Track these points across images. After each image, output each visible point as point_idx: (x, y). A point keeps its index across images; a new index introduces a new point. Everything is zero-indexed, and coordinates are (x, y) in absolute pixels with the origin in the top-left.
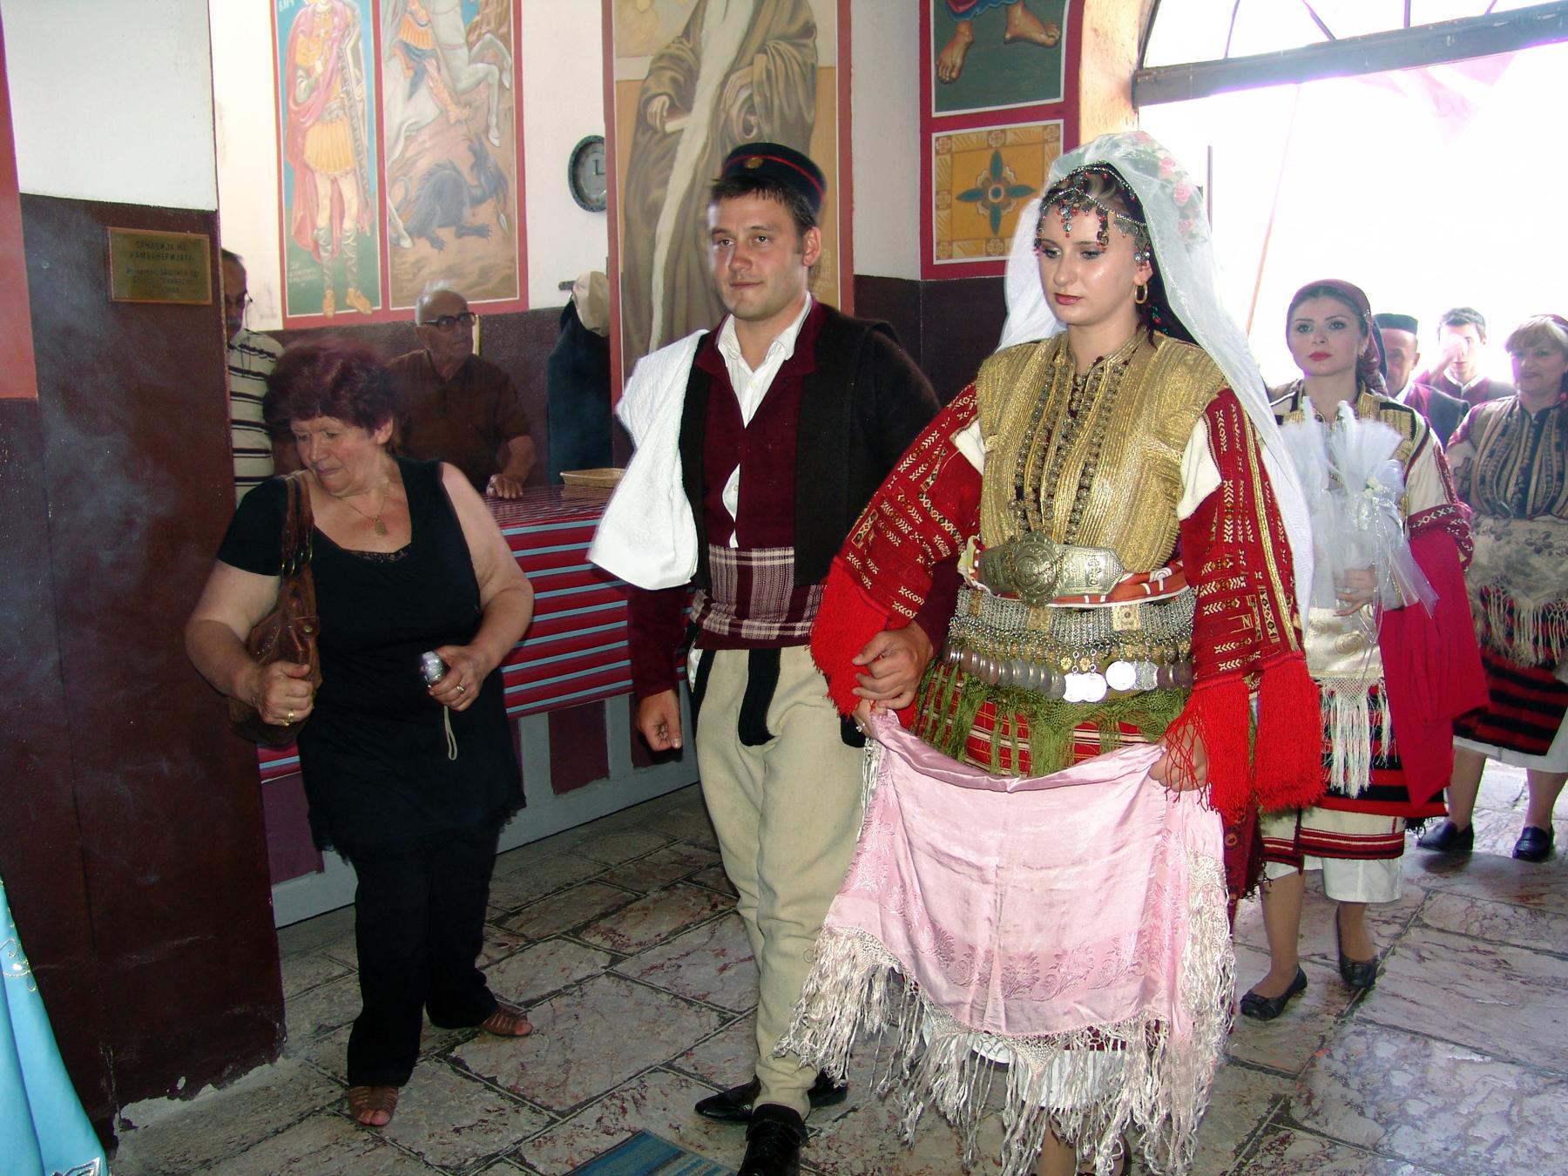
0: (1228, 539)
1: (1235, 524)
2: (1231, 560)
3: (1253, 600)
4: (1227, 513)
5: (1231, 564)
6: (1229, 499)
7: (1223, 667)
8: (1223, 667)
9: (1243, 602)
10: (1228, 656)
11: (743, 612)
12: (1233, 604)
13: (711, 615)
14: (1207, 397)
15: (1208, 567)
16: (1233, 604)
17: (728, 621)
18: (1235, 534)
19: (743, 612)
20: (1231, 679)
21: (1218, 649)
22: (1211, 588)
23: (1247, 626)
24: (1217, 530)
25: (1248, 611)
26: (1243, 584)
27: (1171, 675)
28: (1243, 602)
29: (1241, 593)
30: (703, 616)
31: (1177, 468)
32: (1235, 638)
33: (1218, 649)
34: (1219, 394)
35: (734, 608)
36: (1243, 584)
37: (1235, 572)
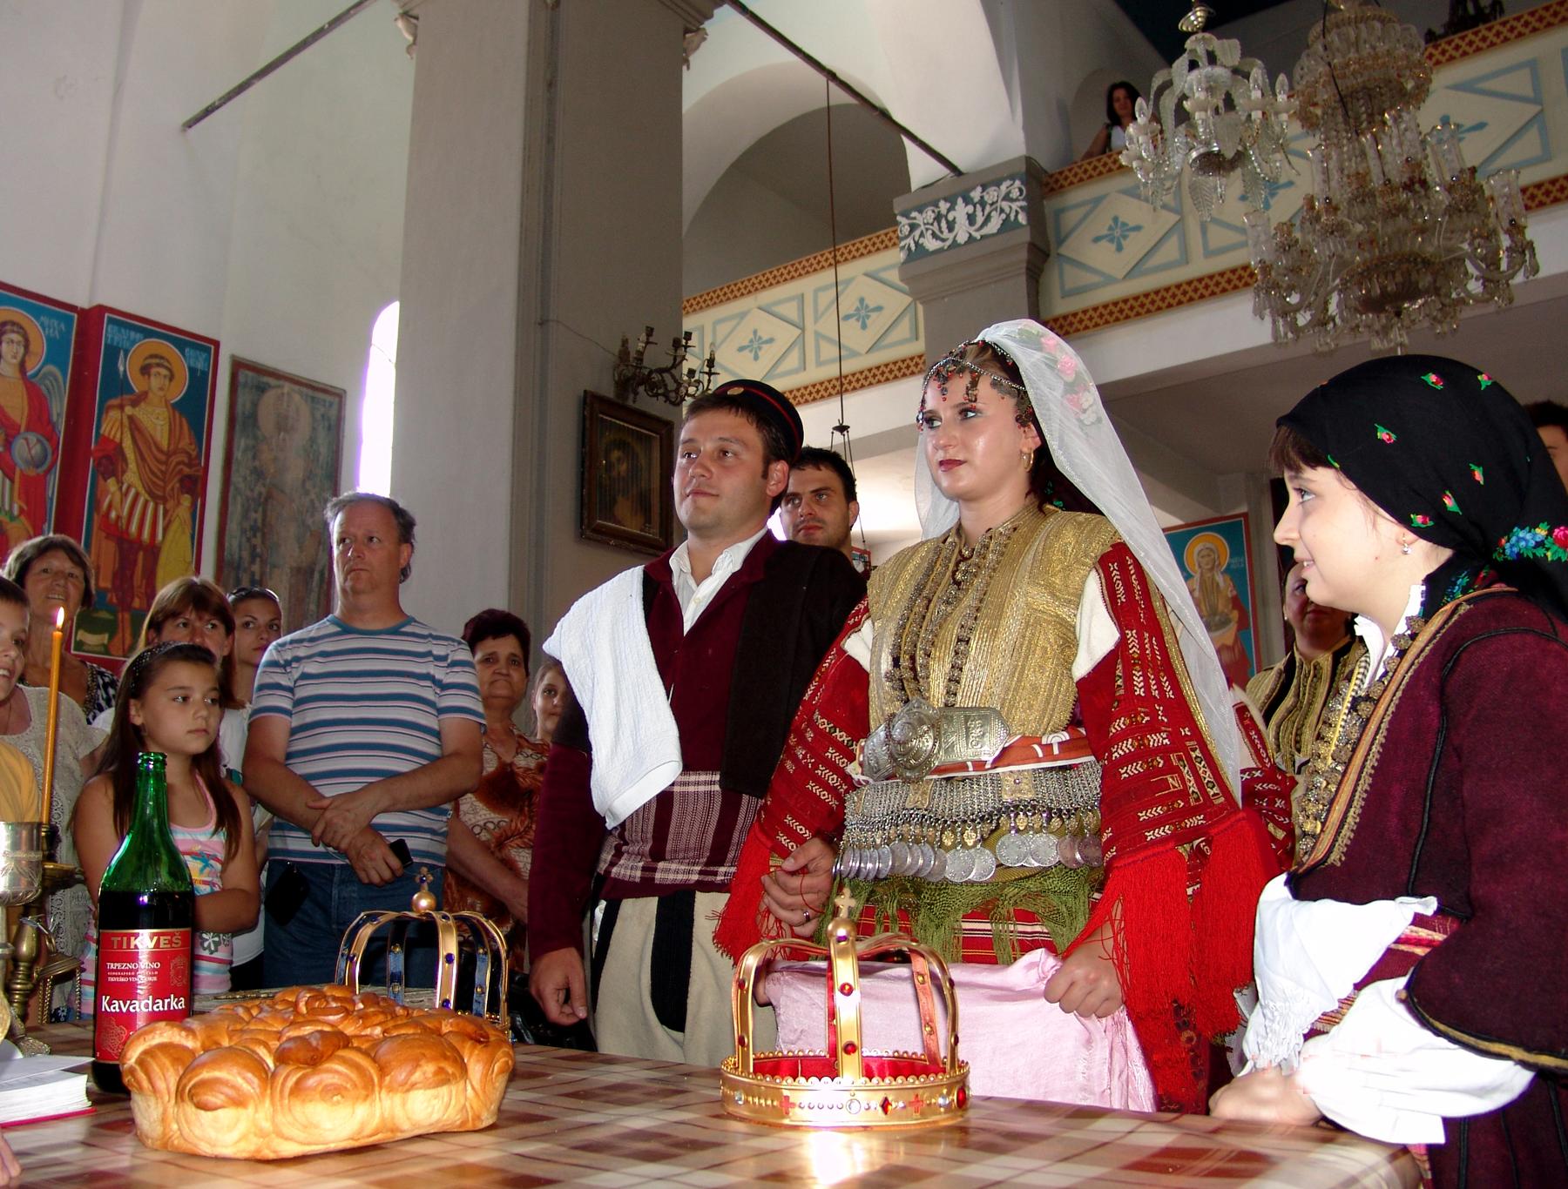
0: (1140, 692)
1: (1146, 680)
2: (1146, 714)
3: (1180, 758)
4: (1135, 664)
5: (1147, 718)
6: (1134, 650)
7: (1150, 835)
8: (1150, 835)
9: (1167, 760)
10: (1155, 823)
11: (658, 853)
12: (1155, 763)
13: (622, 862)
14: (1099, 547)
15: (1120, 724)
16: (1155, 763)
17: (641, 864)
18: (1147, 687)
19: (658, 853)
20: (1161, 849)
21: (1143, 816)
22: (1127, 746)
23: (1174, 787)
24: (1124, 682)
25: (1176, 770)
26: (1166, 741)
27: (1078, 856)
28: (1167, 760)
29: (1163, 751)
30: (613, 864)
31: (1071, 629)
32: (1161, 802)
33: (1143, 816)
34: (1112, 546)
35: (647, 848)
36: (1166, 741)
37: (1154, 727)
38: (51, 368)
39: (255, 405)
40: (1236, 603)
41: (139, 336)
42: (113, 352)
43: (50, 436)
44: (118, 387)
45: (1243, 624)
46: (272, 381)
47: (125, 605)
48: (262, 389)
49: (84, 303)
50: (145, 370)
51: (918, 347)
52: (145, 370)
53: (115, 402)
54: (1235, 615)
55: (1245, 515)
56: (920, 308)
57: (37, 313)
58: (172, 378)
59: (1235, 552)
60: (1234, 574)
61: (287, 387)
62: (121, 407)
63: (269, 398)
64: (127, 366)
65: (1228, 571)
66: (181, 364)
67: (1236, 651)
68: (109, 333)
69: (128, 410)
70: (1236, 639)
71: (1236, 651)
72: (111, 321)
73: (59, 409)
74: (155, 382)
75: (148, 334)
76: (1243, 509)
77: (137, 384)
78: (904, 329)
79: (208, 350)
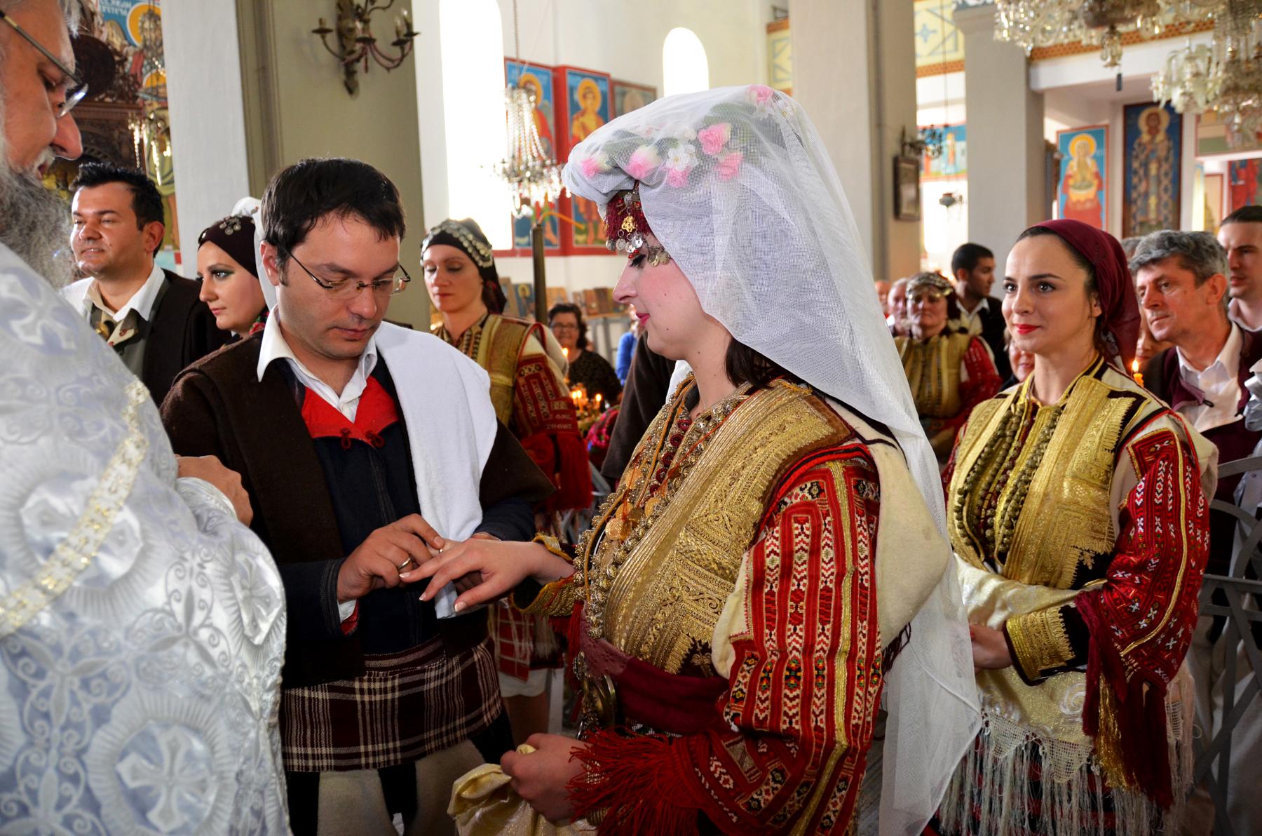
38: (546, 102)
39: (622, 102)
40: (1098, 175)
41: (578, 78)
42: (572, 89)
43: (549, 137)
44: (576, 107)
45: (1100, 187)
46: (627, 89)
47: (590, 219)
48: (624, 94)
49: (551, 62)
50: (584, 96)
51: (959, 55)
52: (584, 96)
53: (575, 116)
54: (1096, 182)
55: (1107, 126)
56: (961, 36)
57: (536, 73)
58: (594, 98)
59: (1099, 145)
60: (1098, 159)
61: (634, 91)
62: (577, 118)
63: (628, 97)
64: (578, 96)
65: (1094, 157)
66: (598, 88)
68: (570, 80)
69: (581, 119)
72: (570, 73)
73: (551, 122)
74: (589, 102)
75: (584, 76)
76: (1106, 122)
77: (582, 105)
78: (950, 44)
79: (604, 80)
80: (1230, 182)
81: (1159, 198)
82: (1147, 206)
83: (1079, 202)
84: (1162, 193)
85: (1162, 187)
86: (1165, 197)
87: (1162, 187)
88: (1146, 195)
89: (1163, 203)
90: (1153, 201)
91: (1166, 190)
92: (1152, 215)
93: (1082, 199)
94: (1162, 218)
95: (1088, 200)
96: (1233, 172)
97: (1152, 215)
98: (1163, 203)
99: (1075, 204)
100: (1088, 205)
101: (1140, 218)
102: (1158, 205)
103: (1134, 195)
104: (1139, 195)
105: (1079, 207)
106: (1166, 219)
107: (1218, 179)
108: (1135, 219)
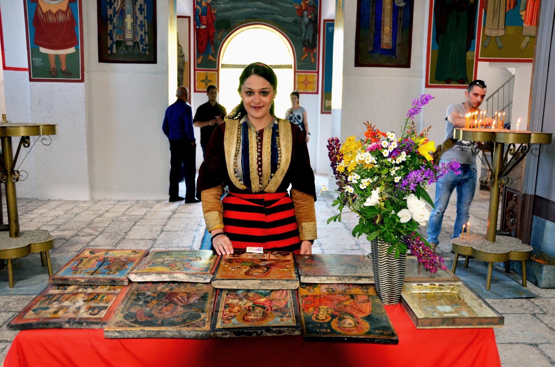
67: (68, 14)
70: (68, 7)
71: (68, 14)
80: (195, 26)
81: (135, 18)
82: (123, 24)
83: (50, 12)
84: (138, 13)
85: (138, 6)
86: (141, 18)
87: (138, 6)
88: (122, 13)
89: (139, 23)
90: (129, 20)
91: (141, 10)
92: (129, 36)
93: (54, 11)
94: (138, 39)
95: (60, 11)
96: (198, 18)
97: (129, 36)
98: (139, 23)
99: (45, 14)
100: (61, 18)
101: (116, 38)
102: (134, 24)
103: (110, 12)
104: (115, 13)
105: (51, 19)
106: (142, 40)
107: (187, 19)
108: (112, 39)
